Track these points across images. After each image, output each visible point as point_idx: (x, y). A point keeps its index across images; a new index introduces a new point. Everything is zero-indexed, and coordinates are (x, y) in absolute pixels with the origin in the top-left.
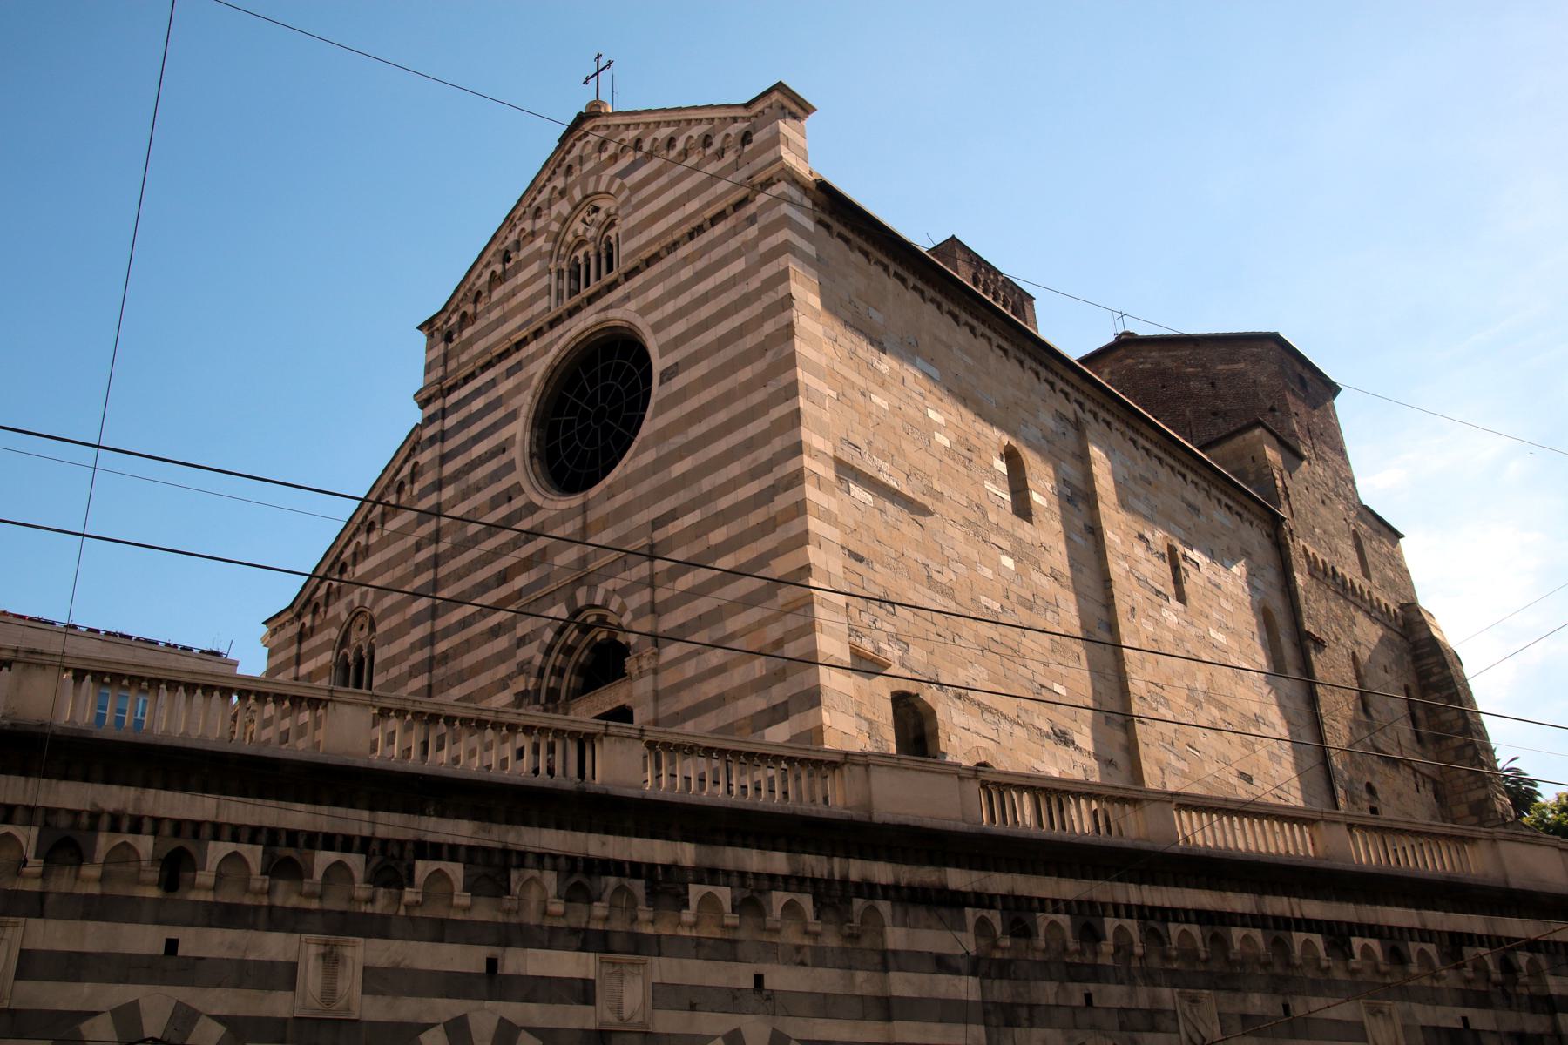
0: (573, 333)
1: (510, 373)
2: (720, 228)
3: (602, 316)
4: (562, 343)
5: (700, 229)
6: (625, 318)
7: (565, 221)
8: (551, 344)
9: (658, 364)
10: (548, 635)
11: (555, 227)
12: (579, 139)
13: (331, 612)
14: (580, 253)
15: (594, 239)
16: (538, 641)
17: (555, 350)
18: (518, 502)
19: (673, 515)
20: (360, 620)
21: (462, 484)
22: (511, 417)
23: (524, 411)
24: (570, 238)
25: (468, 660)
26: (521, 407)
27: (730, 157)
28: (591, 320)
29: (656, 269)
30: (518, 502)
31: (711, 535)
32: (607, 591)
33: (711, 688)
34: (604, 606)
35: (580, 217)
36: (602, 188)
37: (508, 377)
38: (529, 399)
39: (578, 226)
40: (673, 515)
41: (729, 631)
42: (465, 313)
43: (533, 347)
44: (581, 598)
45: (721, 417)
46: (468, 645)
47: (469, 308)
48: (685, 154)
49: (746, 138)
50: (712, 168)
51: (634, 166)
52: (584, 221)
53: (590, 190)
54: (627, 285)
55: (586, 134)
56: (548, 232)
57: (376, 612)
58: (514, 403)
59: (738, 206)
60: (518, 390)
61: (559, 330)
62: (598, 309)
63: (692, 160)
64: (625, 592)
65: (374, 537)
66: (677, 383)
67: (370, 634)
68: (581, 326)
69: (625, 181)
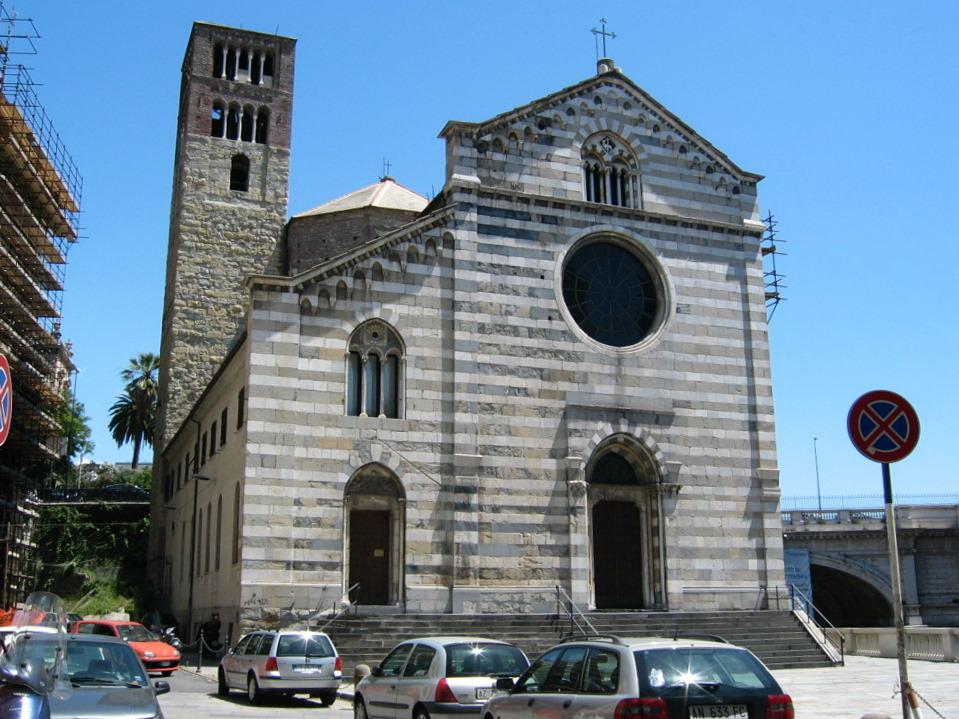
0: (604, 228)
1: (544, 219)
2: (717, 236)
3: (628, 233)
4: (596, 228)
5: (703, 227)
6: (647, 247)
7: (592, 135)
8: (586, 224)
9: (675, 299)
10: (597, 440)
11: (585, 135)
12: (607, 84)
13: (341, 306)
14: (592, 163)
15: (607, 163)
16: (588, 440)
17: (587, 231)
18: (557, 325)
19: (687, 405)
20: (374, 328)
21: (500, 279)
22: (551, 256)
23: (561, 258)
24: (589, 148)
25: (515, 421)
26: (559, 252)
27: (722, 192)
28: (621, 230)
29: (671, 230)
30: (557, 325)
31: (714, 431)
32: (644, 431)
33: (714, 522)
34: (641, 441)
35: (600, 138)
36: (625, 135)
37: (543, 222)
38: (566, 252)
39: (596, 141)
40: (687, 405)
41: (726, 494)
42: (497, 140)
43: (567, 214)
44: (624, 428)
45: (721, 360)
46: (514, 410)
47: (505, 142)
48: (695, 165)
49: (736, 191)
50: (709, 190)
51: (650, 141)
52: (601, 143)
53: (615, 129)
54: (650, 224)
55: (610, 85)
56: (578, 133)
57: (404, 333)
58: (551, 248)
59: (732, 231)
60: (557, 239)
61: (591, 218)
62: (626, 225)
63: (695, 173)
64: (658, 439)
65: (395, 267)
66: (690, 319)
67: (390, 346)
68: (610, 228)
69: (645, 146)
